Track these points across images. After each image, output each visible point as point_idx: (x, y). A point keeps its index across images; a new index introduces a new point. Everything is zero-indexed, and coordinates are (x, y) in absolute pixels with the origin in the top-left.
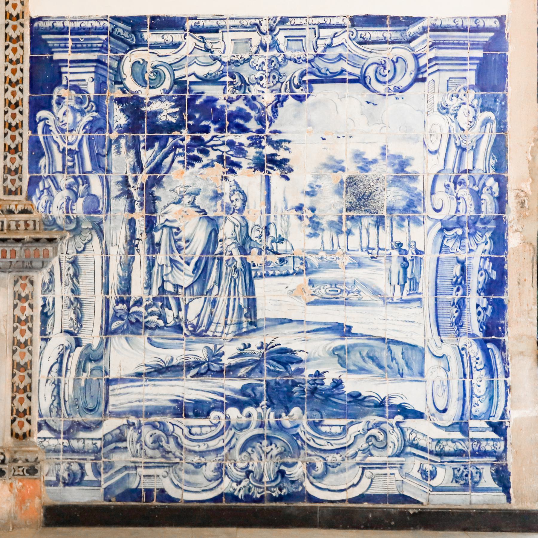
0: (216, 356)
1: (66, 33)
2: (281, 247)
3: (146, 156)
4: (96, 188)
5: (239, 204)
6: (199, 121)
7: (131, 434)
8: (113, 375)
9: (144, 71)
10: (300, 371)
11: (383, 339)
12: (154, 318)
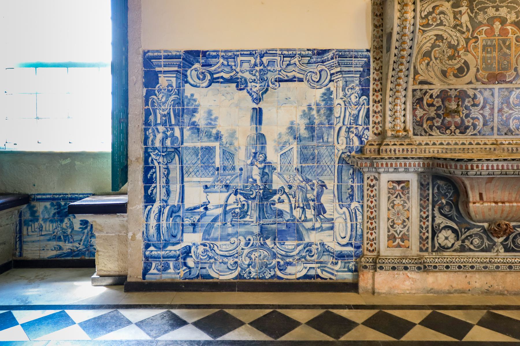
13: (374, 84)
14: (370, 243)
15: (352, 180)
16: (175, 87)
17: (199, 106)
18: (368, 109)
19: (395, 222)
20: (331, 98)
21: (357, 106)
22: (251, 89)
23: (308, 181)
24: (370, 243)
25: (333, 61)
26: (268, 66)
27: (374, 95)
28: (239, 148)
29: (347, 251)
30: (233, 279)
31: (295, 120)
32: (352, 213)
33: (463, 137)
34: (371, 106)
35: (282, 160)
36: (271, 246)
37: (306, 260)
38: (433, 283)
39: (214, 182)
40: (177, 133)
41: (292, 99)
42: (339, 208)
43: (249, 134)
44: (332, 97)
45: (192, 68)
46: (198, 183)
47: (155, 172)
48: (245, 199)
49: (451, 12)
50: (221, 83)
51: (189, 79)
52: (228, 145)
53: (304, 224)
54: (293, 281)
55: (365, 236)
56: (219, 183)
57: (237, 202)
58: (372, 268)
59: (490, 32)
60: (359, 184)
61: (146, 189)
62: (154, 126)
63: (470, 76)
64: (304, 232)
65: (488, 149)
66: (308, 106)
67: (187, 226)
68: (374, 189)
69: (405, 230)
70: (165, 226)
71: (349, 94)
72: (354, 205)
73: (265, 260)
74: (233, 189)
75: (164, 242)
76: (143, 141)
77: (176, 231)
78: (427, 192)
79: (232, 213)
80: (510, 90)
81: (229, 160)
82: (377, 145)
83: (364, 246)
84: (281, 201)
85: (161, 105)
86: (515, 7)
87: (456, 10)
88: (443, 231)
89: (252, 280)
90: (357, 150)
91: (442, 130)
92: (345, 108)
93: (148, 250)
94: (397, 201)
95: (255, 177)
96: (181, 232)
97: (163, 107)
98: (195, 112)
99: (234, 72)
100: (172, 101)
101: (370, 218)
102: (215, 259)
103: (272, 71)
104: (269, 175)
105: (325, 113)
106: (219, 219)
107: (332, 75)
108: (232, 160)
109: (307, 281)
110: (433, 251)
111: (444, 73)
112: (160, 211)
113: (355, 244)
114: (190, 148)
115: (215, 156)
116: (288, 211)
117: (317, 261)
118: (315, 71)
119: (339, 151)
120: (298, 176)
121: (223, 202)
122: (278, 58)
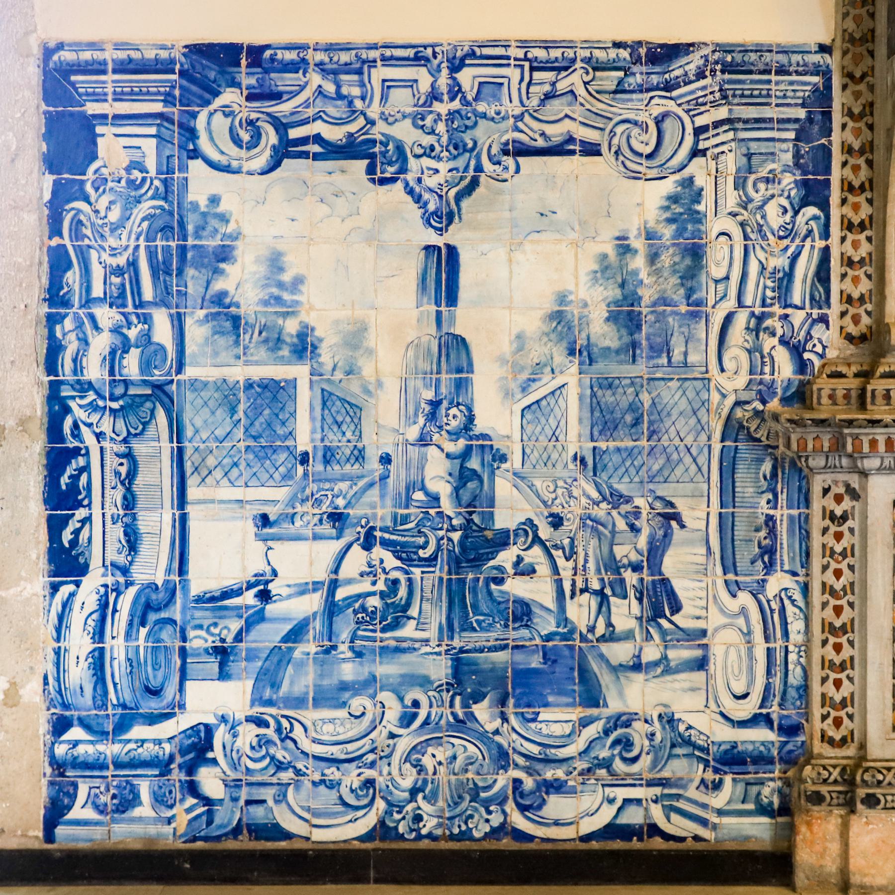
13: (844, 164)
14: (833, 714)
15: (771, 496)
16: (153, 172)
17: (236, 238)
18: (826, 251)
20: (698, 212)
21: (786, 242)
22: (419, 180)
23: (617, 499)
24: (833, 714)
25: (702, 83)
26: (477, 99)
27: (844, 201)
28: (379, 384)
29: (753, 742)
30: (360, 839)
31: (571, 287)
32: (772, 611)
34: (834, 240)
35: (529, 429)
36: (490, 727)
37: (611, 773)
39: (291, 503)
40: (163, 333)
41: (561, 215)
43: (412, 335)
44: (701, 208)
45: (212, 107)
46: (235, 506)
47: (86, 469)
48: (398, 563)
50: (316, 157)
51: (204, 143)
52: (339, 375)
53: (604, 648)
54: (568, 846)
55: (817, 690)
56: (308, 507)
57: (370, 572)
58: (841, 801)
60: (795, 512)
61: (55, 526)
62: (81, 307)
64: (605, 679)
66: (618, 238)
67: (199, 655)
68: (844, 528)
70: (123, 657)
71: (758, 198)
72: (777, 582)
73: (470, 775)
74: (359, 529)
75: (120, 711)
76: (42, 360)
77: (160, 674)
79: (355, 612)
81: (344, 427)
82: (856, 375)
83: (812, 728)
84: (525, 571)
85: (107, 234)
89: (425, 844)
90: (789, 393)
92: (745, 246)
93: (65, 737)
95: (433, 486)
96: (176, 679)
97: (112, 242)
98: (224, 260)
99: (361, 121)
100: (143, 220)
101: (833, 630)
102: (298, 772)
103: (493, 119)
104: (481, 481)
105: (675, 264)
106: (311, 632)
107: (699, 131)
108: (352, 427)
109: (618, 845)
112: (103, 605)
113: (781, 718)
114: (206, 384)
115: (293, 414)
116: (549, 601)
117: (651, 776)
118: (642, 117)
119: (724, 396)
120: (583, 483)
121: (322, 574)
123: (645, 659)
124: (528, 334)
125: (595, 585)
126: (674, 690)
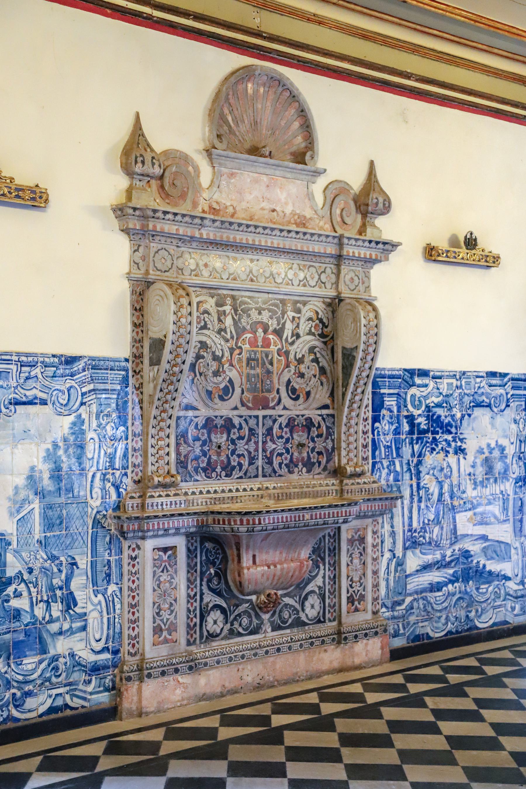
0: (444, 556)
1: (385, 378)
2: (464, 496)
3: (416, 447)
4: (398, 468)
5: (449, 473)
6: (435, 428)
7: (415, 604)
8: (408, 572)
9: (415, 400)
10: (472, 561)
11: (497, 541)
12: (421, 539)
19: (162, 606)
21: (113, 442)
23: (53, 558)
24: (132, 642)
25: (84, 373)
29: (102, 660)
31: (36, 464)
33: (228, 481)
35: (20, 529)
37: (51, 683)
38: (206, 685)
41: (32, 432)
42: (93, 596)
49: (216, 311)
53: (49, 626)
54: (34, 721)
55: (126, 633)
59: (253, 343)
60: (117, 557)
63: (235, 400)
64: (49, 640)
65: (255, 497)
68: (135, 562)
69: (172, 617)
72: (112, 588)
78: (195, 560)
80: (273, 418)
82: (139, 497)
83: (124, 650)
84: (18, 595)
86: (276, 311)
87: (220, 309)
88: (212, 612)
91: (208, 473)
94: (164, 577)
103: (5, 388)
107: (83, 394)
109: (53, 716)
110: (201, 643)
111: (209, 393)
113: (113, 647)
116: (28, 609)
118: (62, 388)
119: (93, 509)
122: (14, 367)
123: (64, 629)
124: (20, 486)
125: (45, 598)
126: (74, 642)
